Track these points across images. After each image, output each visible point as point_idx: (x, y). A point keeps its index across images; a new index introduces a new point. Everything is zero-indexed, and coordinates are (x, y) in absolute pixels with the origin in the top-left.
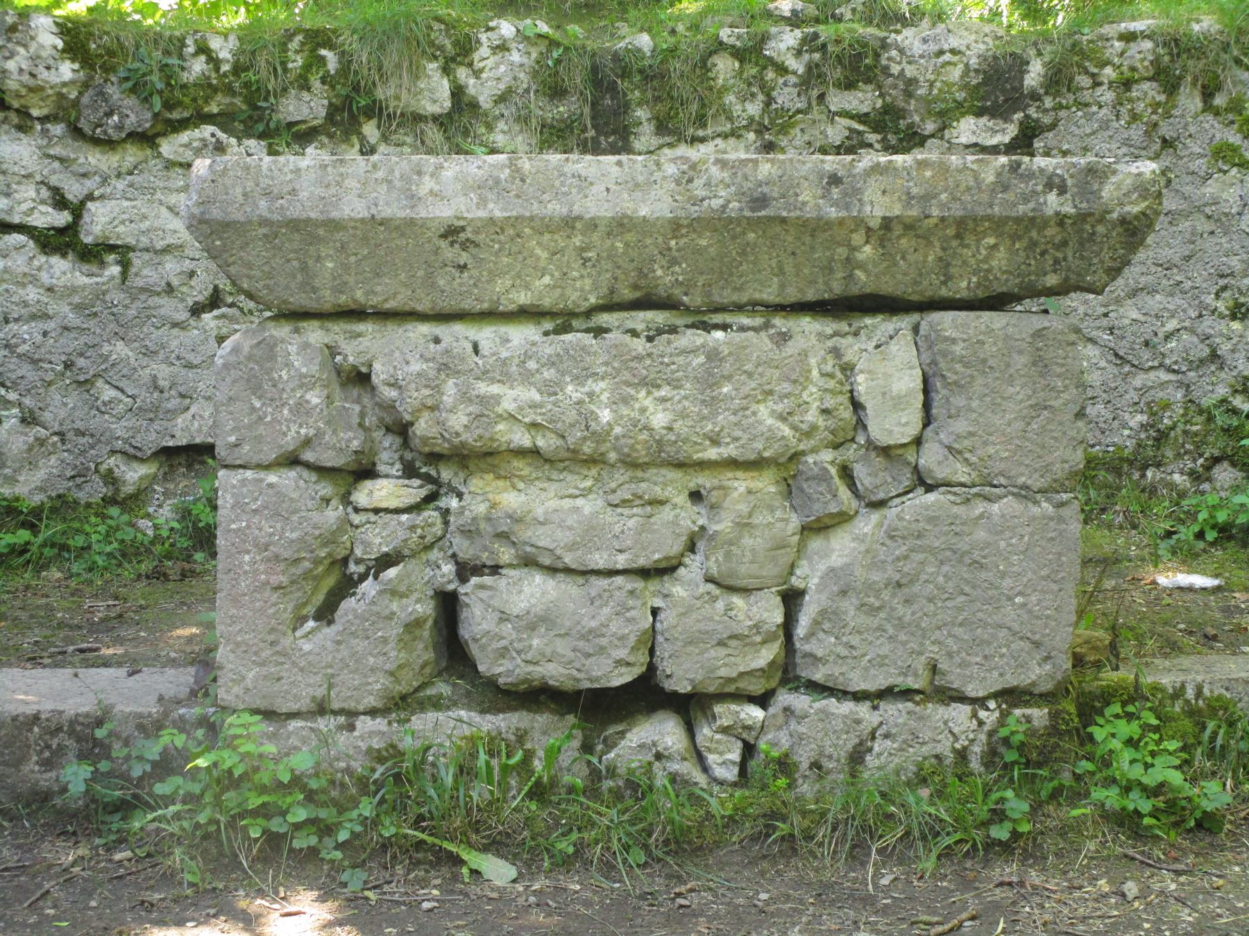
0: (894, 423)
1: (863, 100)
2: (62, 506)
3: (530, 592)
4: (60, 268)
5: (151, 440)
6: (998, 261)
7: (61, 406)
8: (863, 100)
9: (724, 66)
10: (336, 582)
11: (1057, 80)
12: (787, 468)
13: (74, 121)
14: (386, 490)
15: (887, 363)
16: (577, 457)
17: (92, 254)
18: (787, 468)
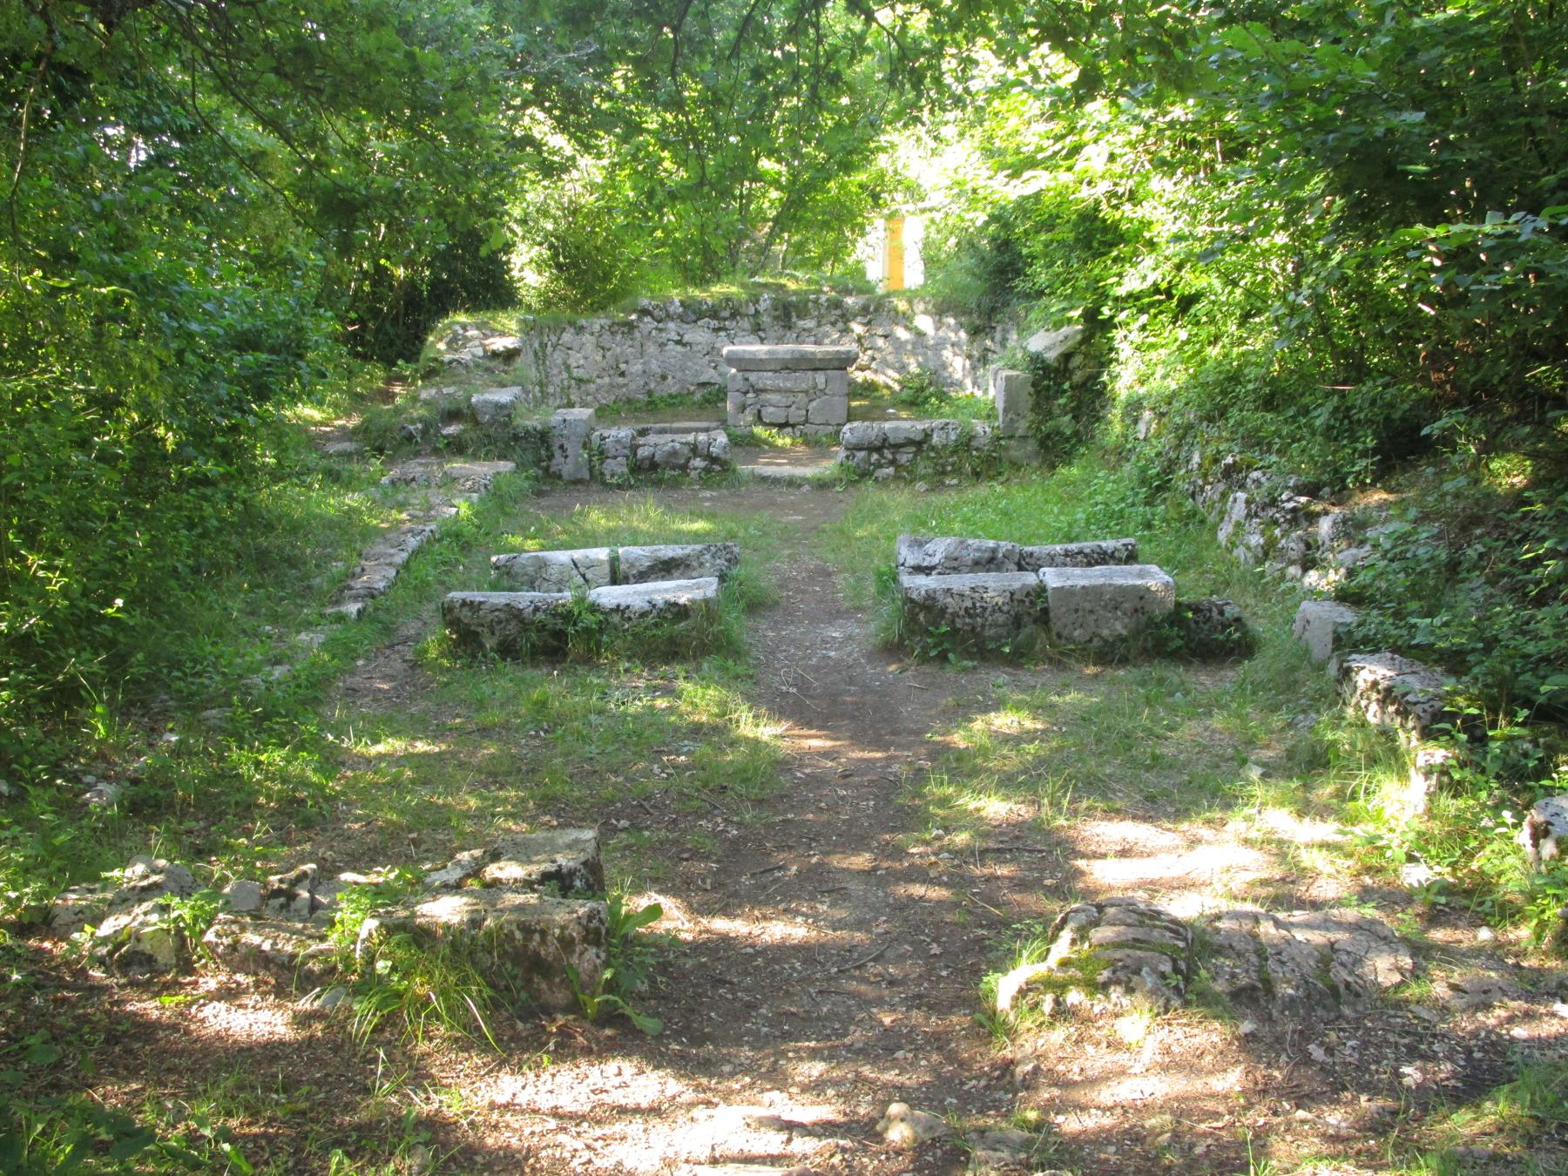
0: (821, 386)
1: (838, 312)
3: (771, 409)
4: (679, 348)
5: (696, 381)
6: (836, 364)
7: (679, 375)
10: (743, 408)
11: (876, 310)
12: (806, 392)
13: (682, 319)
14: (750, 395)
15: (820, 378)
16: (778, 390)
17: (684, 345)
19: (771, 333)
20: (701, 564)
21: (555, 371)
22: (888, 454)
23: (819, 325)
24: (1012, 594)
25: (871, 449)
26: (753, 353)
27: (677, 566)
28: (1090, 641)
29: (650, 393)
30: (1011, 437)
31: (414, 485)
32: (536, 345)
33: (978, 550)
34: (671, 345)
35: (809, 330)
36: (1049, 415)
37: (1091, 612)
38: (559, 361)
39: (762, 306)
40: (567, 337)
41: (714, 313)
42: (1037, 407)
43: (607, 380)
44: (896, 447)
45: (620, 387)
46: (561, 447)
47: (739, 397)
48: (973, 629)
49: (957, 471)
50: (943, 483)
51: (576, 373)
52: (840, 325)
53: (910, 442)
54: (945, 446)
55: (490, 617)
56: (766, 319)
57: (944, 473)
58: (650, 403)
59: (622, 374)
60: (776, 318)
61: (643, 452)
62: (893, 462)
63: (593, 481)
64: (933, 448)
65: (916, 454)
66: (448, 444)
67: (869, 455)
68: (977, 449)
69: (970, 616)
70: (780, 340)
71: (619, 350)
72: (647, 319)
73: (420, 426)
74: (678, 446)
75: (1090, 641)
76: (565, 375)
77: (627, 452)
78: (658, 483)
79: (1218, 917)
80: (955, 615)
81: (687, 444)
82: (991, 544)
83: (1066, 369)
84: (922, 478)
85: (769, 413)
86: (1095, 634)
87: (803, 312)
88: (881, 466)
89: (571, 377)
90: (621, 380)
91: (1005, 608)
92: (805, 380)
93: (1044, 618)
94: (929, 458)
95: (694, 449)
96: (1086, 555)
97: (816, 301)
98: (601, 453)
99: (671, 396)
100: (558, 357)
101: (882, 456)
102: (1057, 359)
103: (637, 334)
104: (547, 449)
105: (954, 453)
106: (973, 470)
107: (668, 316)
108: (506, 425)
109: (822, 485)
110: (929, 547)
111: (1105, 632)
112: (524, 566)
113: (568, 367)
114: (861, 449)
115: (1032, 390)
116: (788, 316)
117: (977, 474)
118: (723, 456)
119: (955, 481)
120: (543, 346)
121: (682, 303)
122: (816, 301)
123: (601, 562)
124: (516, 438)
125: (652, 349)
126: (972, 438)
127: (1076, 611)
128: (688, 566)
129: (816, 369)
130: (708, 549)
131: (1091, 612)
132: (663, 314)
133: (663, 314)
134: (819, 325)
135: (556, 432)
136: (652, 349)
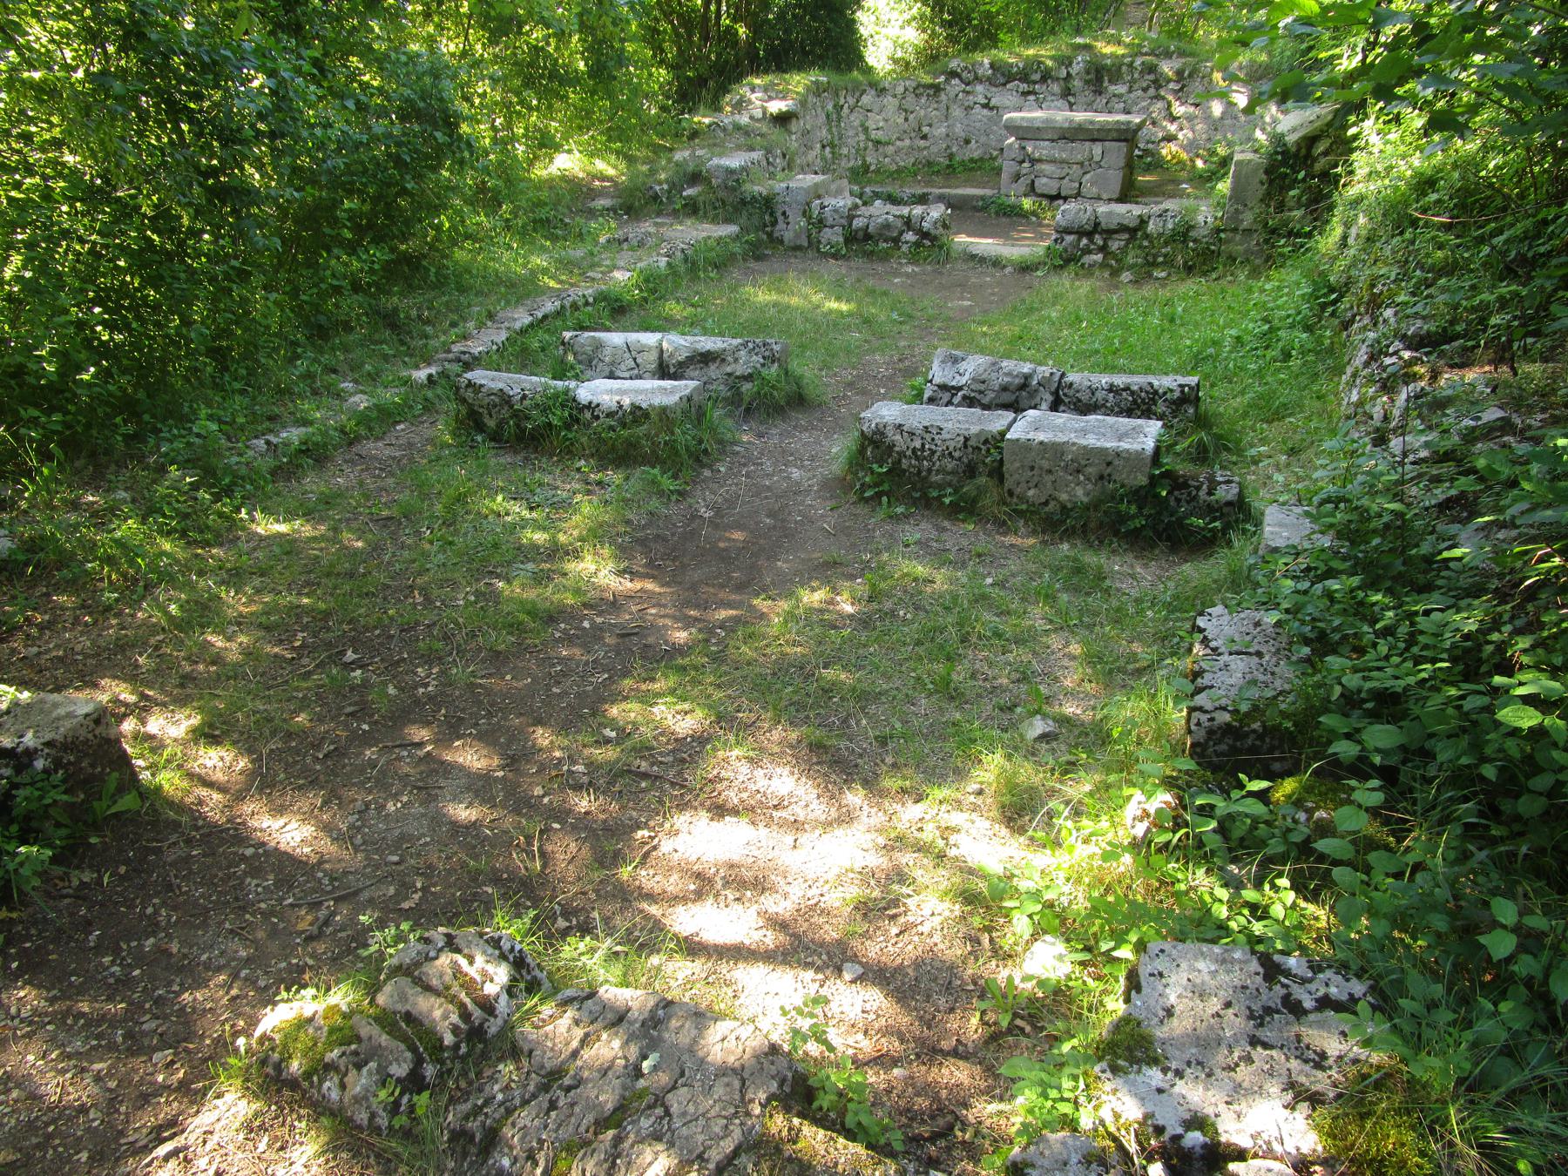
0: (1097, 158)
1: (1152, 77)
2: (981, 159)
3: (1044, 180)
4: (985, 111)
6: (1115, 135)
7: (983, 139)
8: (1152, 77)
9: (1124, 68)
10: (1017, 177)
11: (1190, 75)
12: (1081, 164)
13: (990, 81)
15: (1097, 149)
16: (1053, 161)
17: (991, 109)
18: (1081, 164)
19: (1081, 99)
20: (736, 360)
21: (851, 133)
22: (1099, 240)
23: (1130, 91)
24: (966, 439)
25: (1081, 233)
26: (1029, 120)
27: (714, 360)
28: (1046, 503)
29: (951, 157)
30: (1235, 230)
31: (625, 246)
32: (830, 107)
33: (1009, 374)
34: (978, 108)
35: (1120, 96)
36: (1281, 207)
37: (1050, 471)
38: (857, 123)
39: (1076, 68)
40: (866, 99)
41: (1024, 76)
42: (1266, 199)
43: (907, 142)
44: (1110, 233)
45: (920, 149)
46: (784, 213)
47: (1014, 167)
48: (919, 472)
49: (1169, 263)
50: (1150, 275)
51: (873, 135)
52: (1152, 92)
53: (1123, 228)
54: (1160, 235)
55: (487, 400)
56: (1077, 83)
57: (1154, 264)
58: (949, 167)
59: (924, 137)
60: (1087, 82)
61: (858, 223)
62: (1103, 249)
63: (809, 248)
64: (1147, 236)
65: (1128, 242)
66: (685, 205)
67: (1079, 240)
68: (1195, 241)
69: (917, 458)
70: (1089, 107)
71: (922, 113)
72: (955, 81)
73: (665, 187)
74: (891, 218)
75: (1046, 503)
76: (862, 137)
77: (844, 222)
78: (869, 255)
79: (198, 1112)
80: (902, 454)
81: (902, 217)
82: (1026, 368)
83: (1308, 155)
84: (1130, 268)
85: (1043, 184)
86: (1052, 498)
87: (1116, 76)
88: (1090, 252)
89: (868, 139)
90: (922, 143)
91: (957, 454)
92: (1080, 151)
93: (998, 473)
94: (1140, 247)
95: (908, 222)
96: (1133, 393)
97: (1131, 65)
98: (821, 221)
99: (972, 160)
100: (855, 119)
101: (1091, 241)
102: (1298, 143)
103: (943, 97)
104: (771, 214)
105: (1166, 244)
106: (1185, 263)
107: (976, 78)
108: (734, 189)
109: (1025, 268)
110: (963, 366)
111: (1064, 497)
112: (583, 345)
113: (866, 130)
114: (1070, 233)
115: (1264, 177)
116: (1099, 80)
117: (1189, 270)
118: (933, 232)
119: (1163, 274)
120: (838, 108)
121: (992, 66)
122: (1131, 65)
123: (650, 348)
124: (743, 202)
125: (957, 112)
126: (1191, 227)
127: (1032, 468)
128: (723, 360)
129: (1094, 140)
130: (745, 345)
131: (1050, 471)
132: (971, 76)
133: (971, 76)
134: (1130, 91)
135: (780, 199)
136: (957, 112)
